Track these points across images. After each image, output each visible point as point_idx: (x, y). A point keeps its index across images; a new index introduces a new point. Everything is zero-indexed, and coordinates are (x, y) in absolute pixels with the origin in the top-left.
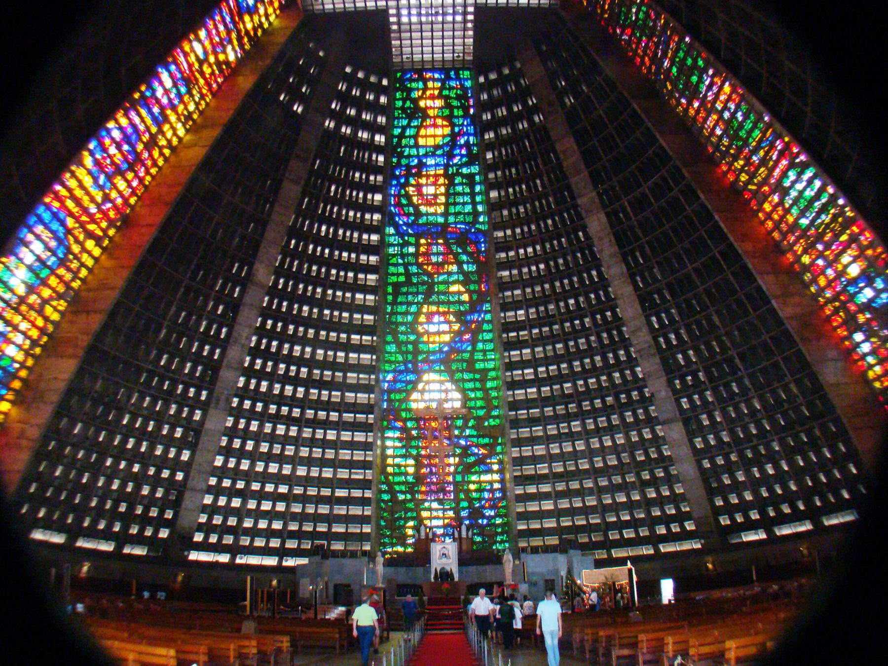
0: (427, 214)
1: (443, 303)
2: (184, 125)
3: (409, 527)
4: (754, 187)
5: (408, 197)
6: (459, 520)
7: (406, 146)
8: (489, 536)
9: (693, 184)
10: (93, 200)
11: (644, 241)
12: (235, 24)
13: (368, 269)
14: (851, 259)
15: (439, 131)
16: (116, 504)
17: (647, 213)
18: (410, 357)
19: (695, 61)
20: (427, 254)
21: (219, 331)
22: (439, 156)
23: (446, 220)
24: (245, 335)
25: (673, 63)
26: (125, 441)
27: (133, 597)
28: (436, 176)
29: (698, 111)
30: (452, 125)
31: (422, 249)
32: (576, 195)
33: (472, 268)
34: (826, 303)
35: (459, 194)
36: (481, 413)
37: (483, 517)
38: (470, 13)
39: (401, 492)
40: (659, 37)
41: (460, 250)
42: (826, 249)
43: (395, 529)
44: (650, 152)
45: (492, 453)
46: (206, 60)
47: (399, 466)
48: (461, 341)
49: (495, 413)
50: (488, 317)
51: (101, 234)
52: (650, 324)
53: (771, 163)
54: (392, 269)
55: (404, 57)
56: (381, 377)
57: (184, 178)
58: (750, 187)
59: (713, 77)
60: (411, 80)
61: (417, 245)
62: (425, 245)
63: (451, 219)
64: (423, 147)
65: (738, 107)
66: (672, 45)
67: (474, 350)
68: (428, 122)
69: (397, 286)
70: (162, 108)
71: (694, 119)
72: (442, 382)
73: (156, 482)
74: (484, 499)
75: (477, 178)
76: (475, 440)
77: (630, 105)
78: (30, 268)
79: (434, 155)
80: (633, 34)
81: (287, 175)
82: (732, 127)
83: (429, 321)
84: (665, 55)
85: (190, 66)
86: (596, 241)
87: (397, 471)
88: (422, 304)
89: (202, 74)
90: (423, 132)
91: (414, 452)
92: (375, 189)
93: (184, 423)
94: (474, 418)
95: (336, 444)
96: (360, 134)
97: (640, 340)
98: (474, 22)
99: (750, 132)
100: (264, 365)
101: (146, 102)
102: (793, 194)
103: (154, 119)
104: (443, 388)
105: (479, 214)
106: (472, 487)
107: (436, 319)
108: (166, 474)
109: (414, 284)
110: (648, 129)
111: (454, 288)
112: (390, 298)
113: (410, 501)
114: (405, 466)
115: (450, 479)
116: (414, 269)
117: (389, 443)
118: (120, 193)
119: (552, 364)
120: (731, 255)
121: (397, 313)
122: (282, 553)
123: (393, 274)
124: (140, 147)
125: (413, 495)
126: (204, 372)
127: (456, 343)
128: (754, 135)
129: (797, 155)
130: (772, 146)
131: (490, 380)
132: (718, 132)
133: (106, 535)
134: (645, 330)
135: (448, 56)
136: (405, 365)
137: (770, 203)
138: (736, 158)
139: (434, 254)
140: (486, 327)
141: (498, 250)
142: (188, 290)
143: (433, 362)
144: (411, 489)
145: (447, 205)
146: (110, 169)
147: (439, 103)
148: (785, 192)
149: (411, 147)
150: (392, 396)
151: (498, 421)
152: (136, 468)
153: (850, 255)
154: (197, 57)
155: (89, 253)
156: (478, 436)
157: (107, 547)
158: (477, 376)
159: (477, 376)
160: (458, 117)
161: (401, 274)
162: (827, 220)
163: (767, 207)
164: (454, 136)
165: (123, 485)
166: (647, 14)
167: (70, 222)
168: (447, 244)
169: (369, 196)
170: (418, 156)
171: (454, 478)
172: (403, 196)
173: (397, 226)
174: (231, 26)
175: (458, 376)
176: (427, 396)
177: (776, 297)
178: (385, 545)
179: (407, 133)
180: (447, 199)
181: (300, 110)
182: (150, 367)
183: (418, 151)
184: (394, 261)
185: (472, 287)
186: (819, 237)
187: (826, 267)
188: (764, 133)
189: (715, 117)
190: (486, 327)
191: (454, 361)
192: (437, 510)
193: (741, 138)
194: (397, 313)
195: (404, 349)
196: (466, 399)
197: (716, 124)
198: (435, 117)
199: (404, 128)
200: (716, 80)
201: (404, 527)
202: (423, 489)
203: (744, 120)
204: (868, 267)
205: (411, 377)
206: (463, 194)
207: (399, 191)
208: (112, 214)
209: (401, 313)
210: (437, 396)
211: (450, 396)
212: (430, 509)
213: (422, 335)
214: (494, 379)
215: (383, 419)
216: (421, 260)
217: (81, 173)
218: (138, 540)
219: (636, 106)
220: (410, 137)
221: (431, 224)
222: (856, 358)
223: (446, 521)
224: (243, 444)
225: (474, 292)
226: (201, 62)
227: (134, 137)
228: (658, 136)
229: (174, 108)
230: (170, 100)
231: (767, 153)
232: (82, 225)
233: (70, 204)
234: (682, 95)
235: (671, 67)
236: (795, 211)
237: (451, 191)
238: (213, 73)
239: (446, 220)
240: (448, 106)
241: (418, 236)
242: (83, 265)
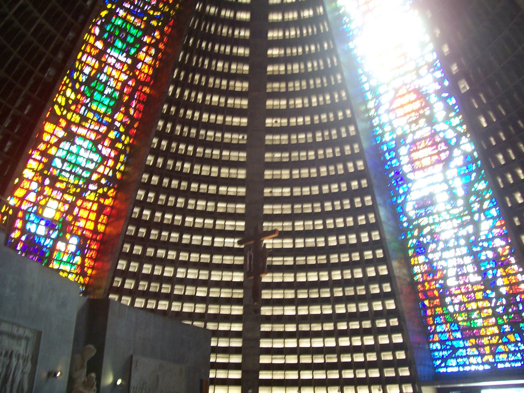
19: (132, 45)
25: (124, 19)
29: (93, 46)
59: (126, 63)
84: (129, 12)
99: (100, 102)
130: (100, 123)
132: (87, 70)
148: (73, 143)
188: (105, 114)
197: (93, 68)
234: (103, 30)
236: (62, 154)
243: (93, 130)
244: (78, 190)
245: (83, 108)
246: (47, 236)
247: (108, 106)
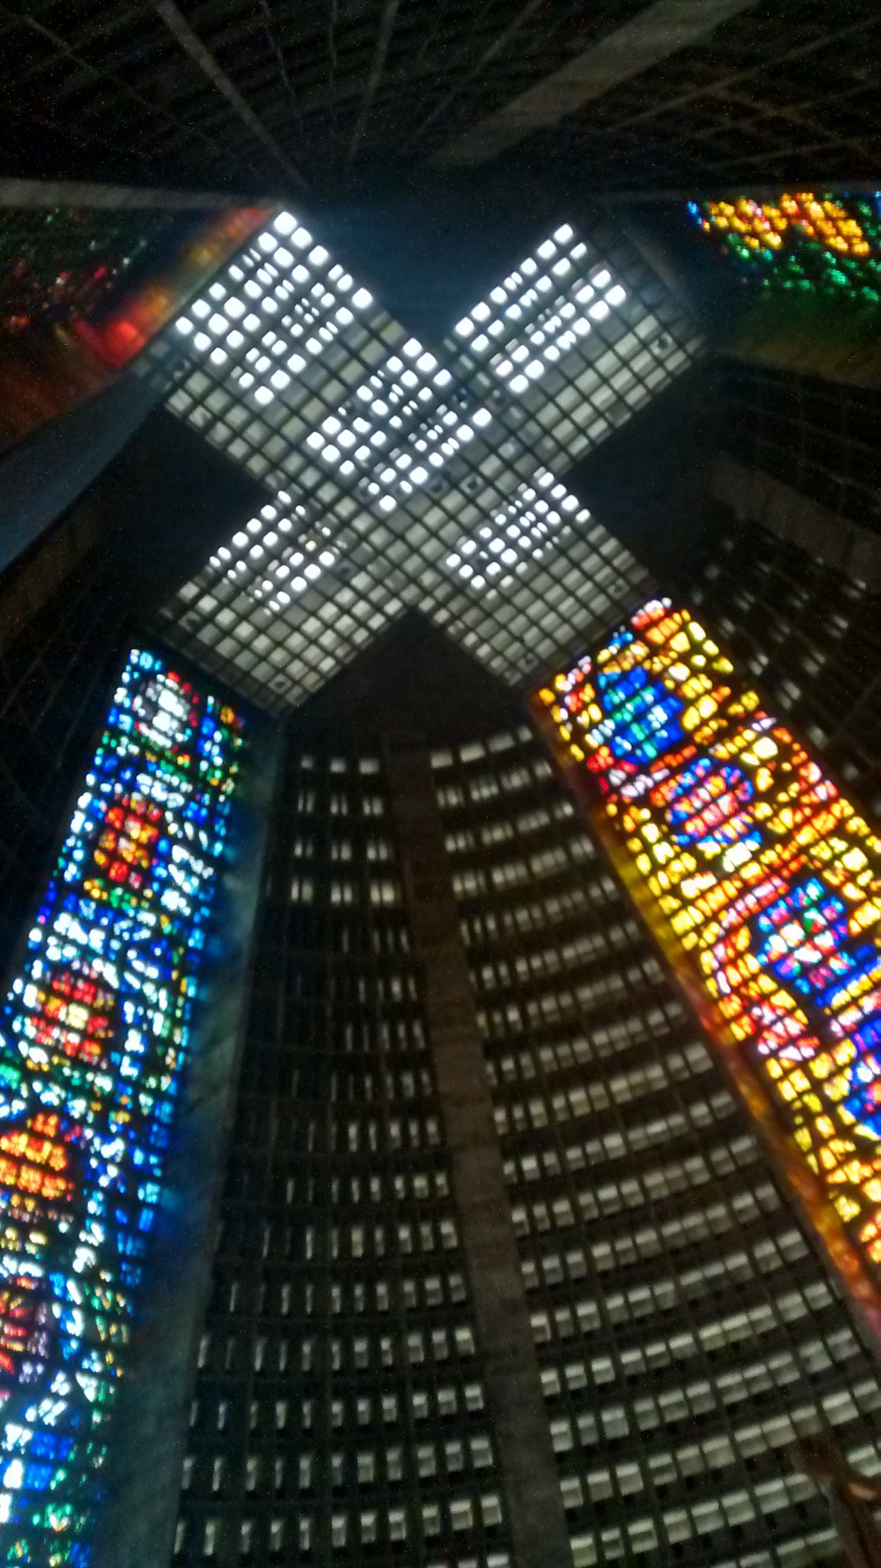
12: (702, 751)
46: (758, 828)
226: (769, 840)
229: (851, 908)
238: (795, 804)
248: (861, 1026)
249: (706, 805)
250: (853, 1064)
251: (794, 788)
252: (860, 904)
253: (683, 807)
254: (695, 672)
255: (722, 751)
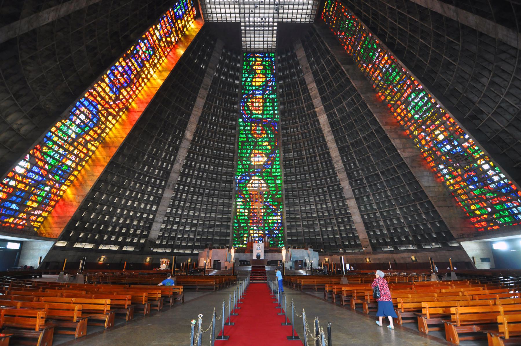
0: (255, 114)
1: (260, 149)
2: (153, 69)
3: (245, 237)
4: (393, 102)
5: (248, 106)
6: (264, 235)
7: (247, 86)
8: (276, 241)
9: (366, 102)
10: (110, 98)
11: (342, 125)
12: (174, 24)
13: (231, 135)
14: (440, 132)
15: (261, 80)
16: (121, 229)
17: (344, 114)
18: (247, 170)
19: (373, 45)
20: (255, 130)
21: (170, 157)
22: (260, 90)
23: (263, 116)
24: (181, 159)
25: (362, 47)
26: (127, 202)
27: (124, 270)
28: (259, 98)
29: (371, 69)
30: (266, 77)
31: (253, 128)
32: (315, 107)
33: (272, 136)
34: (424, 152)
35: (268, 106)
36: (274, 193)
37: (274, 233)
38: (275, 26)
39: (242, 223)
40: (357, 35)
41: (267, 129)
42: (426, 128)
43: (239, 238)
44: (348, 88)
45: (278, 209)
47: (242, 212)
48: (268, 165)
49: (279, 193)
50: (278, 155)
51: (115, 114)
52: (343, 159)
53: (403, 91)
54: (241, 136)
55: (247, 46)
56: (236, 177)
57: (155, 92)
58: (391, 102)
60: (250, 57)
61: (251, 126)
62: (253, 126)
63: (265, 116)
64: (254, 86)
65: (390, 65)
66: (363, 39)
67: (272, 168)
68: (257, 76)
69: (243, 142)
70: (142, 60)
71: (369, 73)
72: (259, 180)
73: (141, 218)
74: (275, 226)
75: (276, 100)
76: (271, 203)
77: (341, 67)
78: (78, 126)
79: (258, 90)
80: (345, 34)
81: (199, 95)
82: (386, 76)
83: (255, 156)
84: (358, 44)
85: (154, 42)
86: (322, 126)
87: (241, 214)
88: (252, 150)
89: (160, 46)
90: (254, 80)
91: (248, 207)
92: (235, 103)
93: (154, 194)
94: (271, 194)
95: (217, 203)
96: (229, 80)
97: (338, 165)
98: (277, 30)
99: (394, 78)
100: (189, 172)
101: (134, 56)
102: (413, 104)
103: (138, 64)
104: (260, 182)
105: (276, 114)
106: (270, 221)
107: (258, 156)
108: (145, 215)
109: (249, 142)
110: (348, 78)
111: (265, 144)
112: (240, 147)
113: (245, 226)
114: (244, 212)
115: (262, 218)
116: (250, 136)
117: (238, 203)
118: (124, 97)
119: (302, 175)
120: (380, 130)
121: (243, 153)
122: (193, 248)
123: (241, 138)
124: (133, 77)
125: (247, 224)
126: (163, 174)
127: (265, 165)
128: (396, 79)
129: (417, 86)
130: (405, 83)
131: (278, 180)
132: (379, 78)
133: (115, 243)
134: (341, 161)
135: (265, 46)
136: (246, 174)
137: (400, 108)
138: (386, 89)
139: (258, 130)
140: (277, 159)
141: (283, 129)
142: (157, 140)
143: (257, 172)
144: (246, 222)
145: (263, 110)
146: (118, 85)
147: (261, 67)
148: (409, 103)
149: (249, 86)
150: (240, 185)
151: (280, 196)
152: (132, 213)
153: (440, 131)
154: (157, 38)
155: (110, 122)
156: (273, 202)
157: (115, 248)
158: (273, 178)
159: (273, 178)
160: (268, 74)
161: (244, 138)
162: (429, 115)
163: (399, 110)
164: (267, 82)
165: (125, 220)
166: (353, 24)
167: (99, 107)
168: (263, 126)
169: (232, 106)
170: (252, 90)
171: (263, 218)
172: (246, 106)
173: (243, 119)
174: (172, 24)
175: (266, 178)
176: (253, 185)
177: (400, 149)
178: (235, 244)
179: (248, 80)
180: (263, 108)
181: (204, 67)
182: (140, 171)
183: (252, 88)
184: (242, 132)
185: (272, 144)
186: (424, 123)
187: (425, 136)
188: (401, 77)
189: (378, 71)
190: (277, 159)
191: (264, 172)
192: (256, 230)
193: (390, 80)
194: (243, 153)
195: (245, 167)
196: (268, 187)
197: (379, 74)
198: (259, 74)
199: (247, 78)
200: (381, 54)
201: (243, 237)
202: (251, 221)
203: (392, 72)
204: (450, 135)
205: (247, 178)
206: (270, 106)
207: (244, 104)
208: (121, 105)
209: (244, 153)
210: (257, 185)
211: (262, 185)
212: (254, 230)
213: (252, 161)
214: (279, 180)
215: (236, 194)
216: (252, 132)
217: (103, 85)
218: (131, 244)
219: (343, 68)
220: (249, 82)
221: (257, 118)
222: (439, 175)
223: (260, 235)
224: (179, 203)
225: (273, 145)
227: (129, 71)
228: (351, 81)
229: (148, 61)
230: (145, 57)
231: (401, 86)
232: (106, 109)
233: (99, 99)
234: (364, 63)
235: (360, 50)
236: (413, 112)
237: (265, 105)
238: (165, 46)
239: (263, 116)
240: (264, 69)
241: (251, 123)
242: (106, 127)
243: (407, 88)
244: (436, 114)
245: (395, 89)
246: (454, 147)
247: (398, 74)
248: (128, 66)
249: (166, 25)
250: (122, 66)
251: (167, 46)
252: (149, 63)
253: (166, 20)
254: (185, 22)
255: (174, 29)
